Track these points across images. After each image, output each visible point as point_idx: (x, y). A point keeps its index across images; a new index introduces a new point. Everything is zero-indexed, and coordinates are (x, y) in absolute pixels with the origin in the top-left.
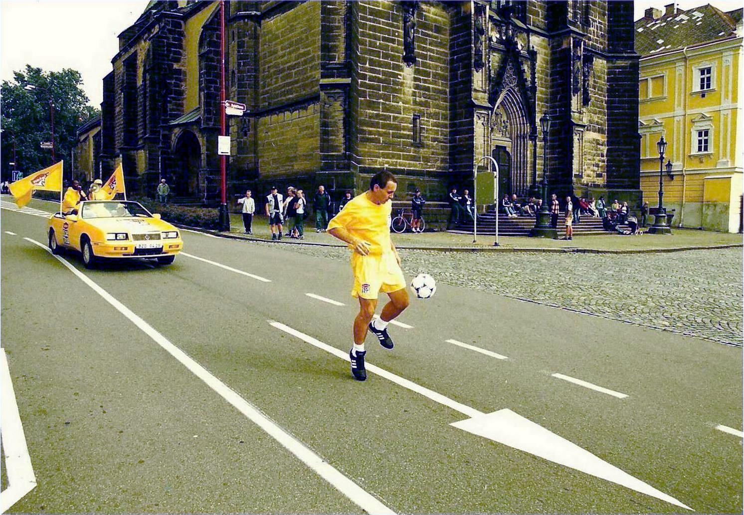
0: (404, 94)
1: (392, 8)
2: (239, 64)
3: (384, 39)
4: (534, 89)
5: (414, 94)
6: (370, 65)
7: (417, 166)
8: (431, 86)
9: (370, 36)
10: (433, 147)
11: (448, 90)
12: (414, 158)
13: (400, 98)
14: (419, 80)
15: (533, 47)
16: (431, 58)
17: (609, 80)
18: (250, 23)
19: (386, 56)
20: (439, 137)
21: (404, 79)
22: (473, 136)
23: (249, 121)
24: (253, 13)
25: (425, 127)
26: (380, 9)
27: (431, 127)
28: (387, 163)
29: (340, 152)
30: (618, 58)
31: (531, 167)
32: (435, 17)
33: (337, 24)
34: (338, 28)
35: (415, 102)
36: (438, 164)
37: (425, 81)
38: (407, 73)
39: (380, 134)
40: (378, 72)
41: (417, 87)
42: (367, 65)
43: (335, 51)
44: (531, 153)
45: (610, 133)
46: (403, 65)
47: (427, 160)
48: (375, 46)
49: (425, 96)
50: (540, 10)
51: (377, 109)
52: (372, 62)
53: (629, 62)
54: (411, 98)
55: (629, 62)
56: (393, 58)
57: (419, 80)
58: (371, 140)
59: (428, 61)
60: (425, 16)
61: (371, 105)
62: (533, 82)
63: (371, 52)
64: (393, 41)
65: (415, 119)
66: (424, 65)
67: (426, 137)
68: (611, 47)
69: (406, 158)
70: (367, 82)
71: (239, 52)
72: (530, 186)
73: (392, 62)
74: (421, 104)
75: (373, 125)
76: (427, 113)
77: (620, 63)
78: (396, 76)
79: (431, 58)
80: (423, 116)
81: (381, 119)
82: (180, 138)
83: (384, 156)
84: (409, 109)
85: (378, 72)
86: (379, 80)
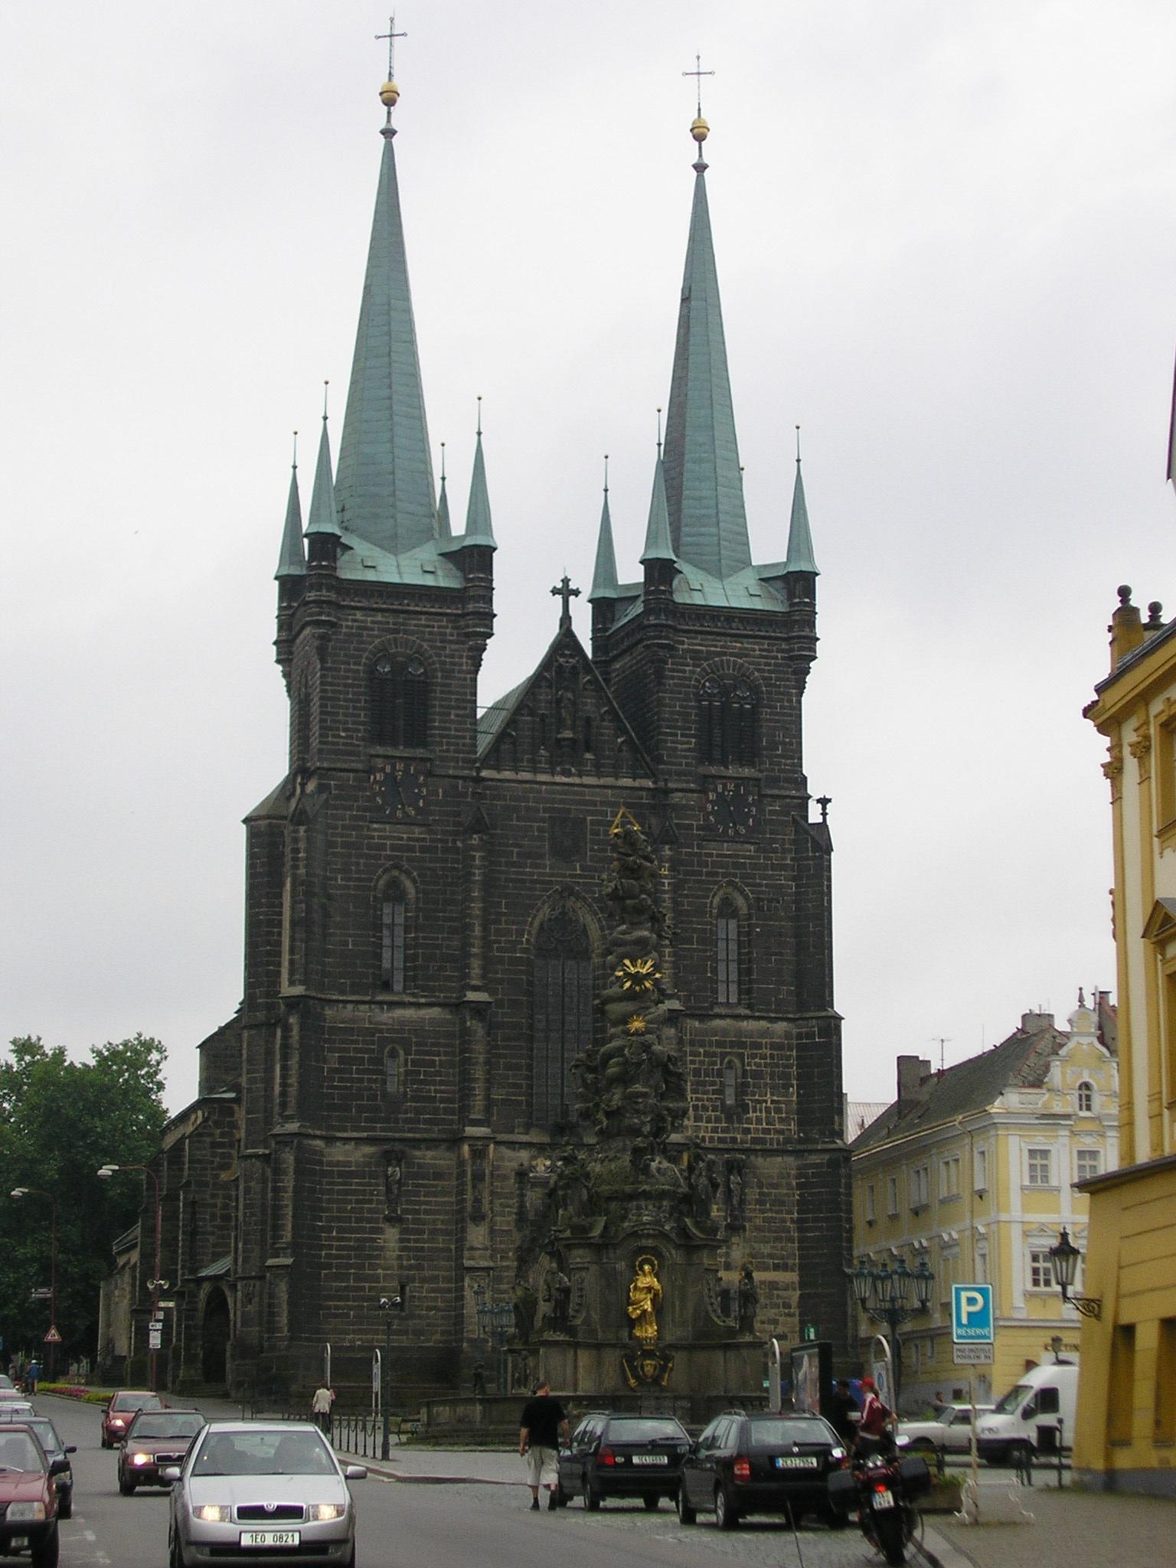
0: (385, 1258)
1: (368, 1164)
2: (245, 1214)
3: (357, 1202)
5: (400, 1258)
6: (337, 1233)
8: (426, 1245)
9: (338, 1201)
10: (428, 1317)
11: (453, 1247)
13: (379, 1264)
14: (408, 1240)
16: (426, 1212)
17: (800, 1186)
18: (258, 1164)
19: (359, 1220)
20: (439, 1304)
21: (385, 1242)
22: (463, 1305)
23: (254, 1286)
24: (261, 1151)
25: (417, 1294)
26: (353, 1169)
27: (424, 1294)
28: (359, 1340)
29: (283, 1332)
30: (810, 1151)
32: (433, 1162)
33: (285, 1203)
34: (287, 1206)
35: (401, 1267)
36: (438, 1337)
37: (416, 1241)
38: (391, 1235)
39: (350, 1308)
40: (349, 1240)
41: (402, 1249)
42: (334, 1234)
43: (284, 1230)
45: (803, 1268)
47: (418, 1333)
48: (345, 1210)
49: (417, 1258)
51: (348, 1280)
52: (340, 1230)
53: (827, 1157)
54: (395, 1263)
55: (827, 1157)
56: (369, 1221)
57: (408, 1240)
58: (336, 1316)
59: (422, 1216)
60: (418, 1164)
61: (338, 1277)
63: (339, 1219)
64: (370, 1202)
65: (403, 1287)
66: (415, 1222)
67: (418, 1306)
68: (802, 1135)
70: (334, 1252)
71: (245, 1200)
73: (368, 1225)
74: (410, 1267)
75: (340, 1298)
76: (420, 1278)
77: (815, 1159)
78: (374, 1240)
79: (426, 1212)
80: (414, 1281)
81: (353, 1291)
82: (210, 1298)
83: (354, 1332)
84: (391, 1275)
85: (349, 1240)
86: (351, 1248)
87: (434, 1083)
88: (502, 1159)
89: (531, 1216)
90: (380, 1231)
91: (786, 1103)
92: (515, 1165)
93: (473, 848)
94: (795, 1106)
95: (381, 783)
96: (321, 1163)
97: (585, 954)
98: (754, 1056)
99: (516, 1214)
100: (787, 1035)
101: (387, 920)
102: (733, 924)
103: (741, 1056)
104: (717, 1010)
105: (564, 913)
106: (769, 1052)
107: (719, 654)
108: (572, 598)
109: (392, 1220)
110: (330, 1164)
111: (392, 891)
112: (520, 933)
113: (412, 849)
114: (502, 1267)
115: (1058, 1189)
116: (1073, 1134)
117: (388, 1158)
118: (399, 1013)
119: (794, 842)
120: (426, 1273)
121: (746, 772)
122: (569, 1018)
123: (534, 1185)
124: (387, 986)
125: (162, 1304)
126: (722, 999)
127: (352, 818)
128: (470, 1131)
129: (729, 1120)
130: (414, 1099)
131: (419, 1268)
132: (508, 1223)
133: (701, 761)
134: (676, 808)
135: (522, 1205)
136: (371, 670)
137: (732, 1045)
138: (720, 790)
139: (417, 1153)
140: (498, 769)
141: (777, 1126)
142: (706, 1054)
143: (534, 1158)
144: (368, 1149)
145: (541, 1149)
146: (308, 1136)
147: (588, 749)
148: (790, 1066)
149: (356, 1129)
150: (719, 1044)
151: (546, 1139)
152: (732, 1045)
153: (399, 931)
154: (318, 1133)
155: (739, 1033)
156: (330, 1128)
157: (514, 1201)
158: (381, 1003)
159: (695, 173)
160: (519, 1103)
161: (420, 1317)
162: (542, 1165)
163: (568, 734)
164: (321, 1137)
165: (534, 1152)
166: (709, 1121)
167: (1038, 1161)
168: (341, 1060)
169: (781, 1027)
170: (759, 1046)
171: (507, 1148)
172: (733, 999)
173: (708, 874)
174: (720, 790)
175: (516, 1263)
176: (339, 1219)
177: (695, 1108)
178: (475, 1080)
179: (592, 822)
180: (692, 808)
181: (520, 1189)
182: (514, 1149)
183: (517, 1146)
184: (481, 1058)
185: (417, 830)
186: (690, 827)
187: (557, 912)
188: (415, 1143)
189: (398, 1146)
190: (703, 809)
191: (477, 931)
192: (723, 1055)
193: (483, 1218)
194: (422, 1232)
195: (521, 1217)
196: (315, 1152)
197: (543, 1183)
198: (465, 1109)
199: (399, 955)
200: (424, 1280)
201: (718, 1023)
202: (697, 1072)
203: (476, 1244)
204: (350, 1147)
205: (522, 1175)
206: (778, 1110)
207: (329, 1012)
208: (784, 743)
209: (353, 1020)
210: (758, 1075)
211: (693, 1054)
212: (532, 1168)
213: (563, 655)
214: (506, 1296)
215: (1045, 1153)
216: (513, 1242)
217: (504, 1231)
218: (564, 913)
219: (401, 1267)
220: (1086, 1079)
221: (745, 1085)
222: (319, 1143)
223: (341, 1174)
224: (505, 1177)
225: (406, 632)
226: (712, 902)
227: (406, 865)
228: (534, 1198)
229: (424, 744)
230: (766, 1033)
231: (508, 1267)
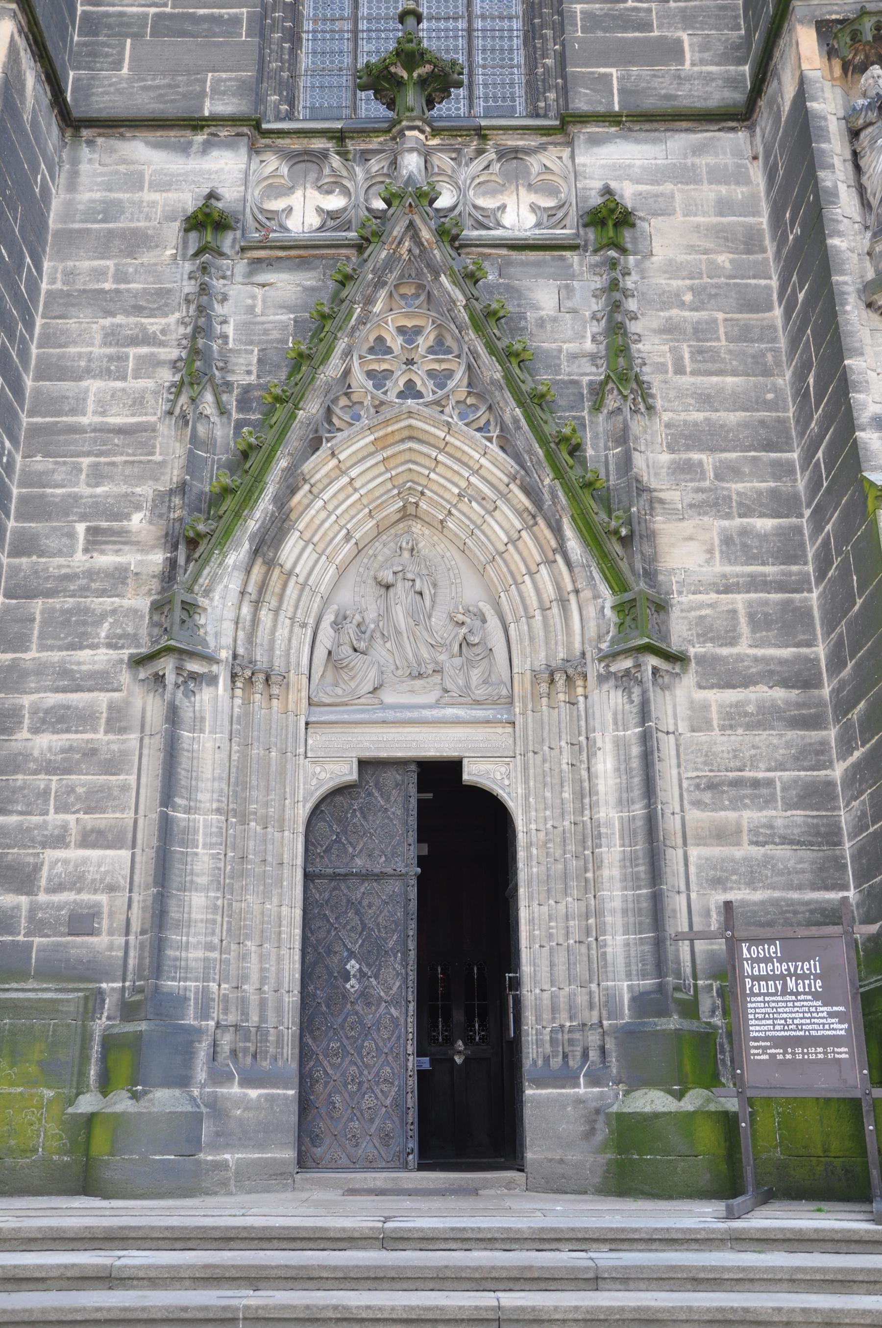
15: (607, 191)
31: (629, 860)
44: (622, 768)
50: (685, 36)
72: (640, 1002)
88: (135, 181)
99: (174, 365)
114: (91, 574)
132: (138, 402)
171: (157, 146)
175: (157, 558)
182: (184, 149)
183: (200, 138)
214: (102, 699)
216: (153, 471)
217: (120, 431)
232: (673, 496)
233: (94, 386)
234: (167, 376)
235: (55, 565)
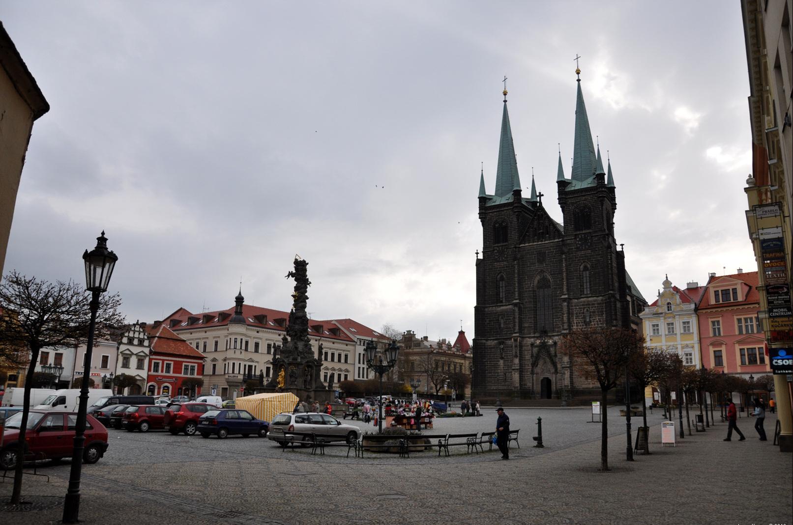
4: (556, 356)
5: (503, 367)
7: (505, 388)
12: (503, 386)
16: (510, 356)
38: (501, 362)
46: (500, 360)
47: (508, 386)
52: (490, 362)
54: (502, 368)
56: (496, 359)
61: (490, 373)
62: (555, 353)
63: (490, 359)
66: (507, 358)
69: (501, 386)
74: (506, 370)
75: (490, 378)
83: (494, 386)
86: (492, 366)
87: (511, 324)
89: (535, 355)
90: (499, 361)
91: (602, 319)
92: (530, 343)
93: (515, 264)
94: (605, 319)
95: (496, 253)
96: (485, 346)
97: (549, 286)
98: (593, 307)
100: (602, 300)
101: (501, 285)
102: (588, 272)
103: (589, 308)
104: (582, 296)
105: (544, 277)
106: (597, 306)
107: (578, 202)
108: (542, 197)
109: (502, 358)
110: (487, 346)
111: (502, 279)
112: (531, 284)
113: (504, 267)
115: (661, 335)
116: (665, 318)
117: (500, 343)
118: (502, 308)
119: (601, 247)
120: (510, 371)
121: (588, 231)
122: (546, 303)
123: (535, 347)
124: (502, 302)
125: (447, 381)
126: (585, 293)
127: (490, 262)
128: (514, 335)
129: (586, 325)
130: (506, 328)
131: (508, 370)
133: (576, 230)
134: (569, 244)
135: (532, 352)
136: (494, 226)
137: (586, 305)
138: (580, 237)
139: (507, 341)
140: (524, 244)
141: (600, 325)
142: (579, 308)
143: (536, 340)
144: (496, 342)
145: (537, 338)
146: (479, 340)
147: (547, 234)
148: (603, 309)
149: (494, 337)
150: (583, 305)
151: (538, 335)
152: (586, 305)
153: (504, 288)
154: (483, 339)
155: (588, 301)
156: (487, 337)
157: (530, 352)
158: (498, 306)
159: (577, 82)
160: (532, 327)
161: (509, 382)
162: (538, 342)
163: (541, 231)
164: (484, 340)
165: (535, 339)
166: (580, 326)
167: (656, 328)
168: (490, 321)
169: (600, 298)
170: (594, 304)
172: (589, 292)
173: (578, 260)
174: (580, 237)
176: (490, 359)
177: (576, 323)
178: (516, 322)
179: (548, 252)
180: (573, 244)
181: (532, 348)
184: (517, 316)
185: (505, 262)
186: (573, 249)
187: (542, 277)
188: (506, 339)
189: (503, 340)
190: (575, 243)
191: (517, 285)
192: (584, 308)
193: (517, 356)
194: (508, 361)
195: (532, 356)
196: (482, 343)
197: (537, 346)
198: (514, 329)
199: (504, 294)
200: (509, 373)
201: (582, 299)
202: (577, 314)
203: (516, 363)
204: (492, 341)
205: (532, 345)
206: (600, 321)
207: (486, 310)
208: (598, 221)
209: (493, 311)
210: (594, 312)
211: (575, 309)
212: (535, 343)
213: (539, 212)
215: (657, 325)
218: (544, 277)
219: (504, 370)
220: (668, 301)
221: (591, 315)
222: (484, 341)
223: (489, 348)
224: (528, 346)
225: (502, 215)
226: (579, 268)
227: (502, 271)
228: (535, 350)
229: (506, 241)
230: (595, 301)
231: (529, 369)
232: (558, 362)
233: (527, 356)
234: (530, 356)
235: (526, 368)
